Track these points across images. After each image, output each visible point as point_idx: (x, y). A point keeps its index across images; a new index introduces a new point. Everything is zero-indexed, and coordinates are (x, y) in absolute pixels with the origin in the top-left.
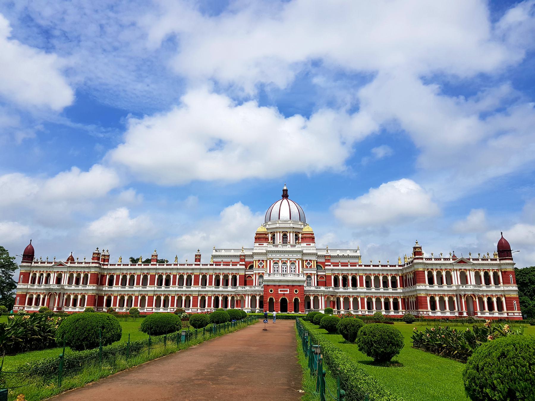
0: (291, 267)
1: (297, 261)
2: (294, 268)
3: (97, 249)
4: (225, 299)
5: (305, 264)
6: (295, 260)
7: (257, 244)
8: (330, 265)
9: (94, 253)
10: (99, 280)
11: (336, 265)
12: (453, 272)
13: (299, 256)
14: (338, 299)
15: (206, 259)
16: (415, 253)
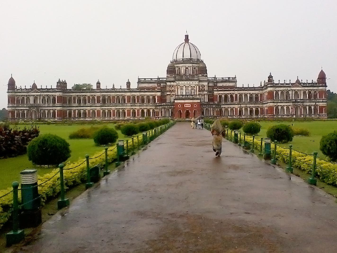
0: (192, 90)
1: (196, 87)
2: (194, 91)
3: (59, 79)
4: (149, 111)
5: (200, 88)
6: (194, 86)
7: (169, 75)
8: (216, 88)
9: (57, 83)
10: (62, 100)
11: (220, 87)
12: (290, 92)
13: (197, 83)
14: (221, 110)
15: (133, 86)
16: (269, 81)
